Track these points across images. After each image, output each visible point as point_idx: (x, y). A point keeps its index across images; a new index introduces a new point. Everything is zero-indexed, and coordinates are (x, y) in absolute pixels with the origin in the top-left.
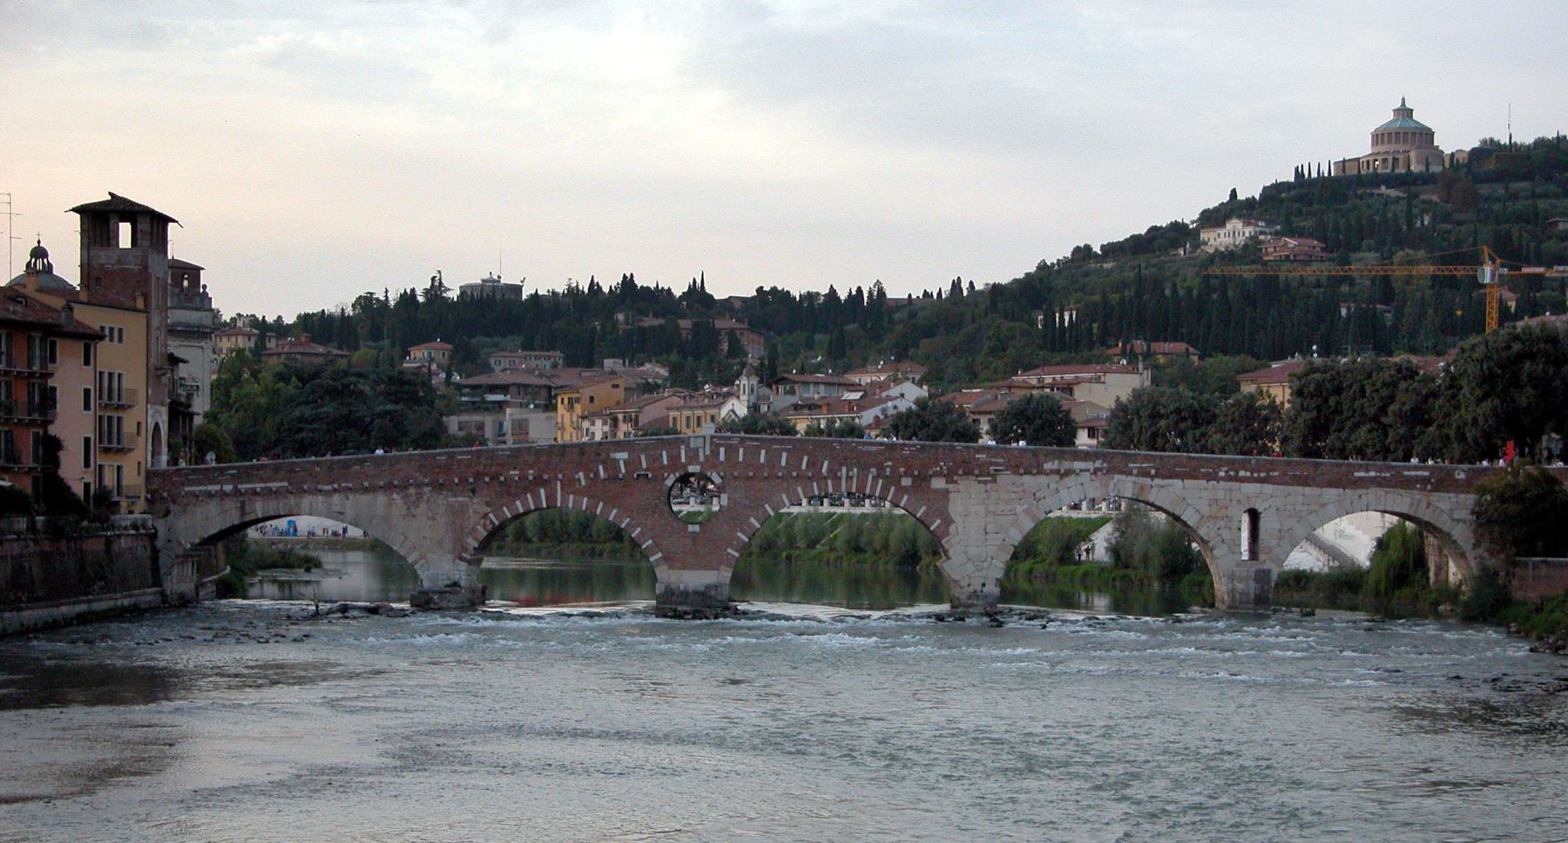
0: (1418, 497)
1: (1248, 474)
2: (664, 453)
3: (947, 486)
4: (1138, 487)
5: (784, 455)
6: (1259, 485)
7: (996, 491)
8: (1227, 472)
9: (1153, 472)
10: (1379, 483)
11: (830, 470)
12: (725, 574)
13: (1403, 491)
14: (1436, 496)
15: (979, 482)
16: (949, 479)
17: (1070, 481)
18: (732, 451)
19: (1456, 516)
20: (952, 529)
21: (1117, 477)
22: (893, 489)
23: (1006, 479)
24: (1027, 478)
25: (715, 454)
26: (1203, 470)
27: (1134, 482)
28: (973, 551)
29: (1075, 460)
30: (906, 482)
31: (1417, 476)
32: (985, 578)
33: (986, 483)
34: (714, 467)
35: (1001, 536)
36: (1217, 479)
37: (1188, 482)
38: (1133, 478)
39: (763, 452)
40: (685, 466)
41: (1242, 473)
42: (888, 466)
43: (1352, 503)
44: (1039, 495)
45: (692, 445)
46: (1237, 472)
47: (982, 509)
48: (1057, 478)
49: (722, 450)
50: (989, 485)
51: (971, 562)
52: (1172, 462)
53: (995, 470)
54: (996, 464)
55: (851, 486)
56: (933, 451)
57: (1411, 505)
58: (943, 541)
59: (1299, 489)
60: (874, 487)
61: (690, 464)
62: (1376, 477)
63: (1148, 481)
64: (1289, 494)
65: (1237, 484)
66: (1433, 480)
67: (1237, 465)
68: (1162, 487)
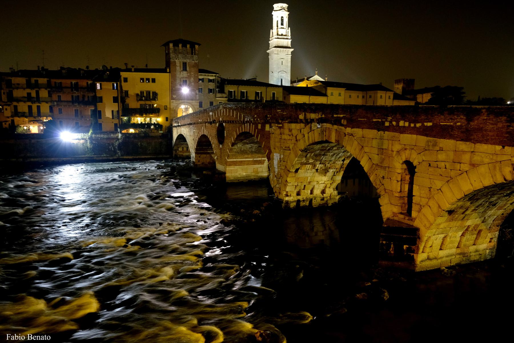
1: (407, 124)
8: (391, 122)
16: (271, 127)
18: (226, 111)
25: (224, 111)
26: (375, 120)
30: (260, 126)
41: (401, 123)
46: (398, 123)
48: (302, 125)
49: (225, 110)
65: (396, 134)
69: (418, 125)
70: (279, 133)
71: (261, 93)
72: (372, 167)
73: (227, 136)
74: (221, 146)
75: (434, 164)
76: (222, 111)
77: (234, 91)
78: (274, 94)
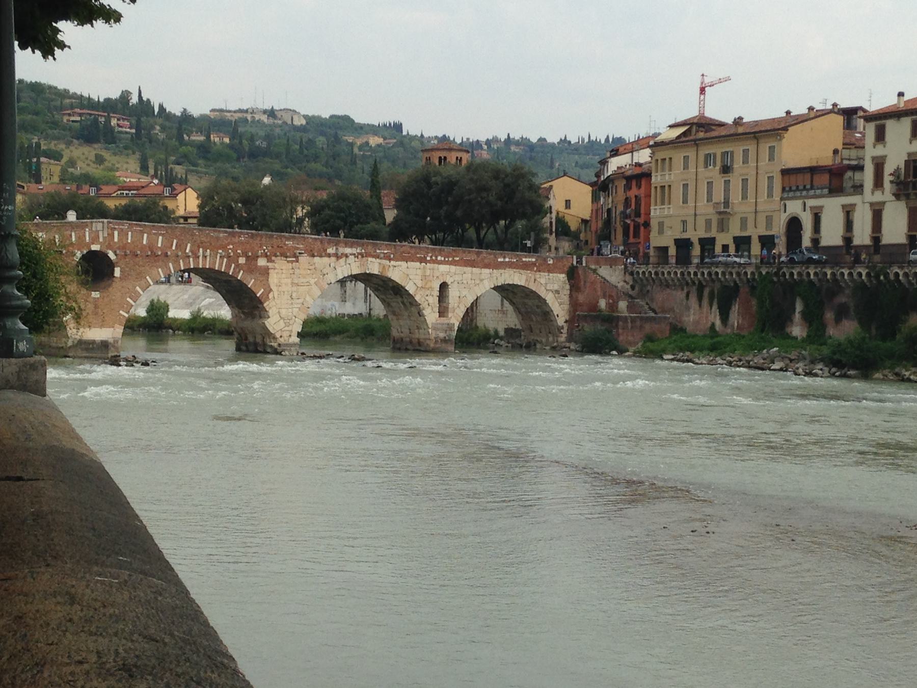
0: (530, 275)
1: (443, 259)
2: (73, 234)
3: (268, 264)
4: (382, 266)
5: (160, 238)
6: (448, 266)
7: (299, 268)
8: (431, 257)
9: (392, 256)
10: (510, 265)
11: (191, 251)
12: (117, 330)
13: (522, 271)
14: (538, 275)
15: (288, 262)
16: (270, 260)
17: (342, 261)
19: (549, 287)
20: (271, 296)
21: (370, 259)
22: (233, 265)
23: (304, 259)
24: (317, 259)
26: (418, 256)
27: (380, 263)
28: (284, 312)
29: (346, 247)
30: (242, 260)
31: (529, 261)
32: (291, 331)
33: (292, 262)
34: (110, 247)
36: (426, 262)
37: (411, 264)
38: (378, 260)
39: (145, 235)
40: (88, 245)
41: (439, 258)
42: (230, 249)
43: (497, 279)
44: (325, 271)
45: (94, 229)
46: (436, 257)
47: (289, 281)
48: (333, 259)
49: (116, 233)
50: (294, 264)
51: (282, 321)
52: (402, 250)
53: (300, 253)
54: (298, 249)
55: (206, 263)
56: (259, 239)
57: (527, 280)
58: (265, 305)
59: (469, 269)
60: (221, 264)
61: (93, 244)
62: (509, 262)
63: (386, 262)
64: (465, 273)
65: (436, 265)
66: (537, 264)
67: (437, 252)
68: (395, 267)
69: (450, 259)
70: (291, 267)
72: (417, 290)
73: (124, 277)
74: (95, 295)
75: (460, 282)
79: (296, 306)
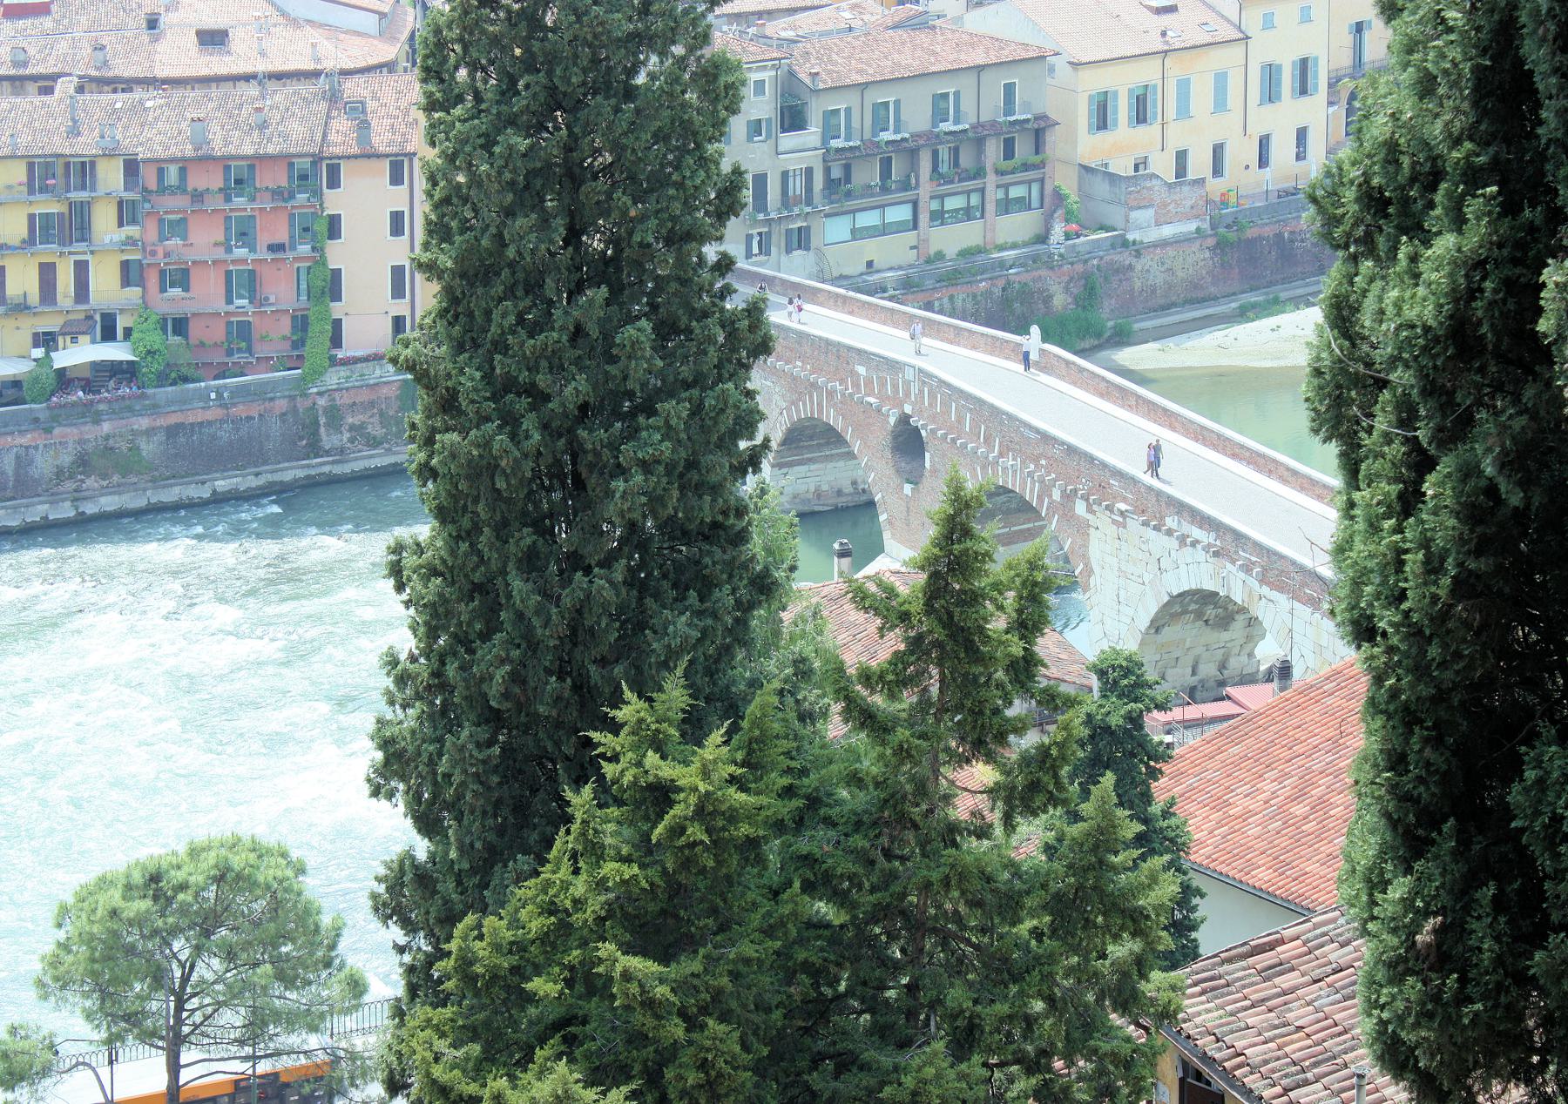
3: (1089, 516)
16: (1090, 510)
23: (1134, 524)
24: (1150, 533)
25: (921, 392)
29: (1192, 523)
30: (1056, 495)
35: (1130, 611)
48: (1175, 544)
60: (1032, 491)
71: (957, 94)
74: (908, 488)
76: (915, 389)
77: (848, 111)
78: (1009, 89)
79: (1124, 619)
